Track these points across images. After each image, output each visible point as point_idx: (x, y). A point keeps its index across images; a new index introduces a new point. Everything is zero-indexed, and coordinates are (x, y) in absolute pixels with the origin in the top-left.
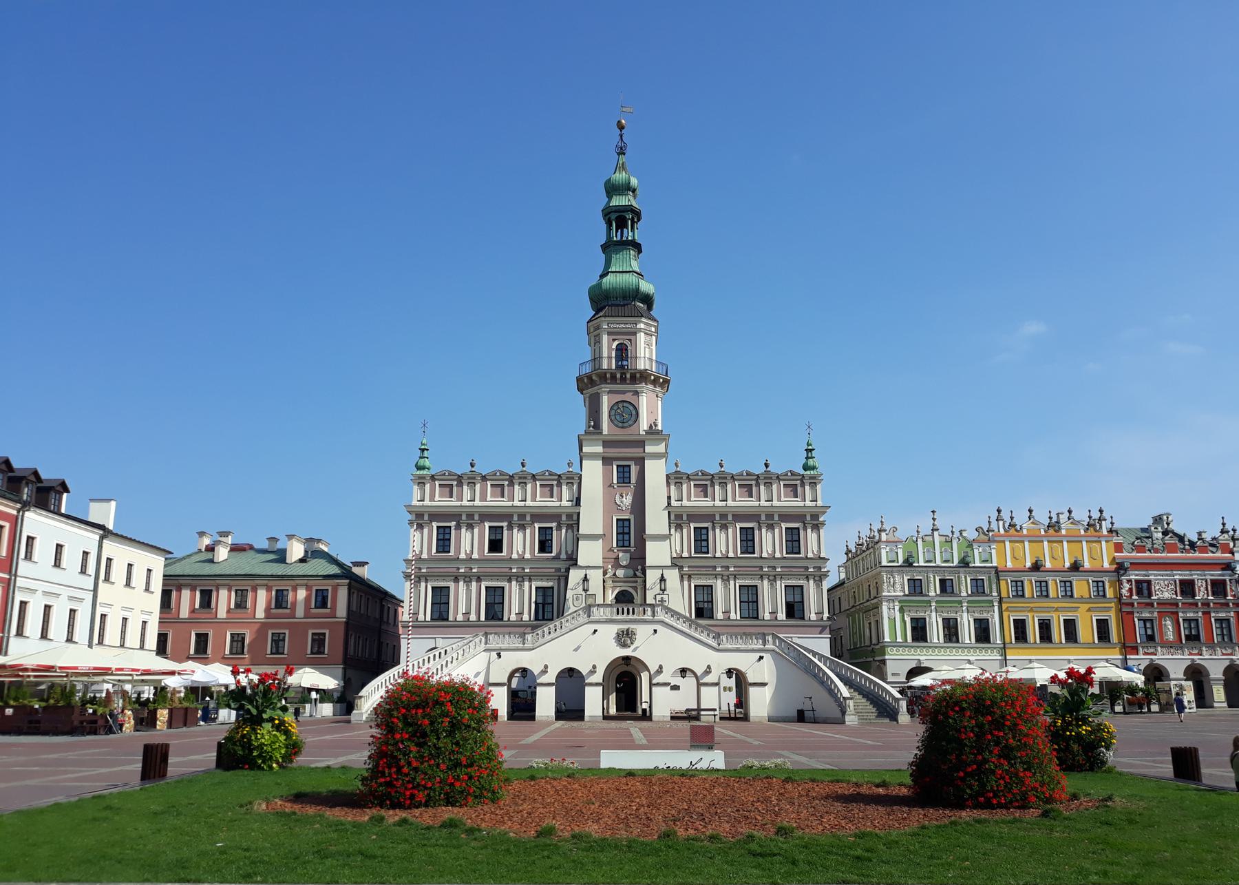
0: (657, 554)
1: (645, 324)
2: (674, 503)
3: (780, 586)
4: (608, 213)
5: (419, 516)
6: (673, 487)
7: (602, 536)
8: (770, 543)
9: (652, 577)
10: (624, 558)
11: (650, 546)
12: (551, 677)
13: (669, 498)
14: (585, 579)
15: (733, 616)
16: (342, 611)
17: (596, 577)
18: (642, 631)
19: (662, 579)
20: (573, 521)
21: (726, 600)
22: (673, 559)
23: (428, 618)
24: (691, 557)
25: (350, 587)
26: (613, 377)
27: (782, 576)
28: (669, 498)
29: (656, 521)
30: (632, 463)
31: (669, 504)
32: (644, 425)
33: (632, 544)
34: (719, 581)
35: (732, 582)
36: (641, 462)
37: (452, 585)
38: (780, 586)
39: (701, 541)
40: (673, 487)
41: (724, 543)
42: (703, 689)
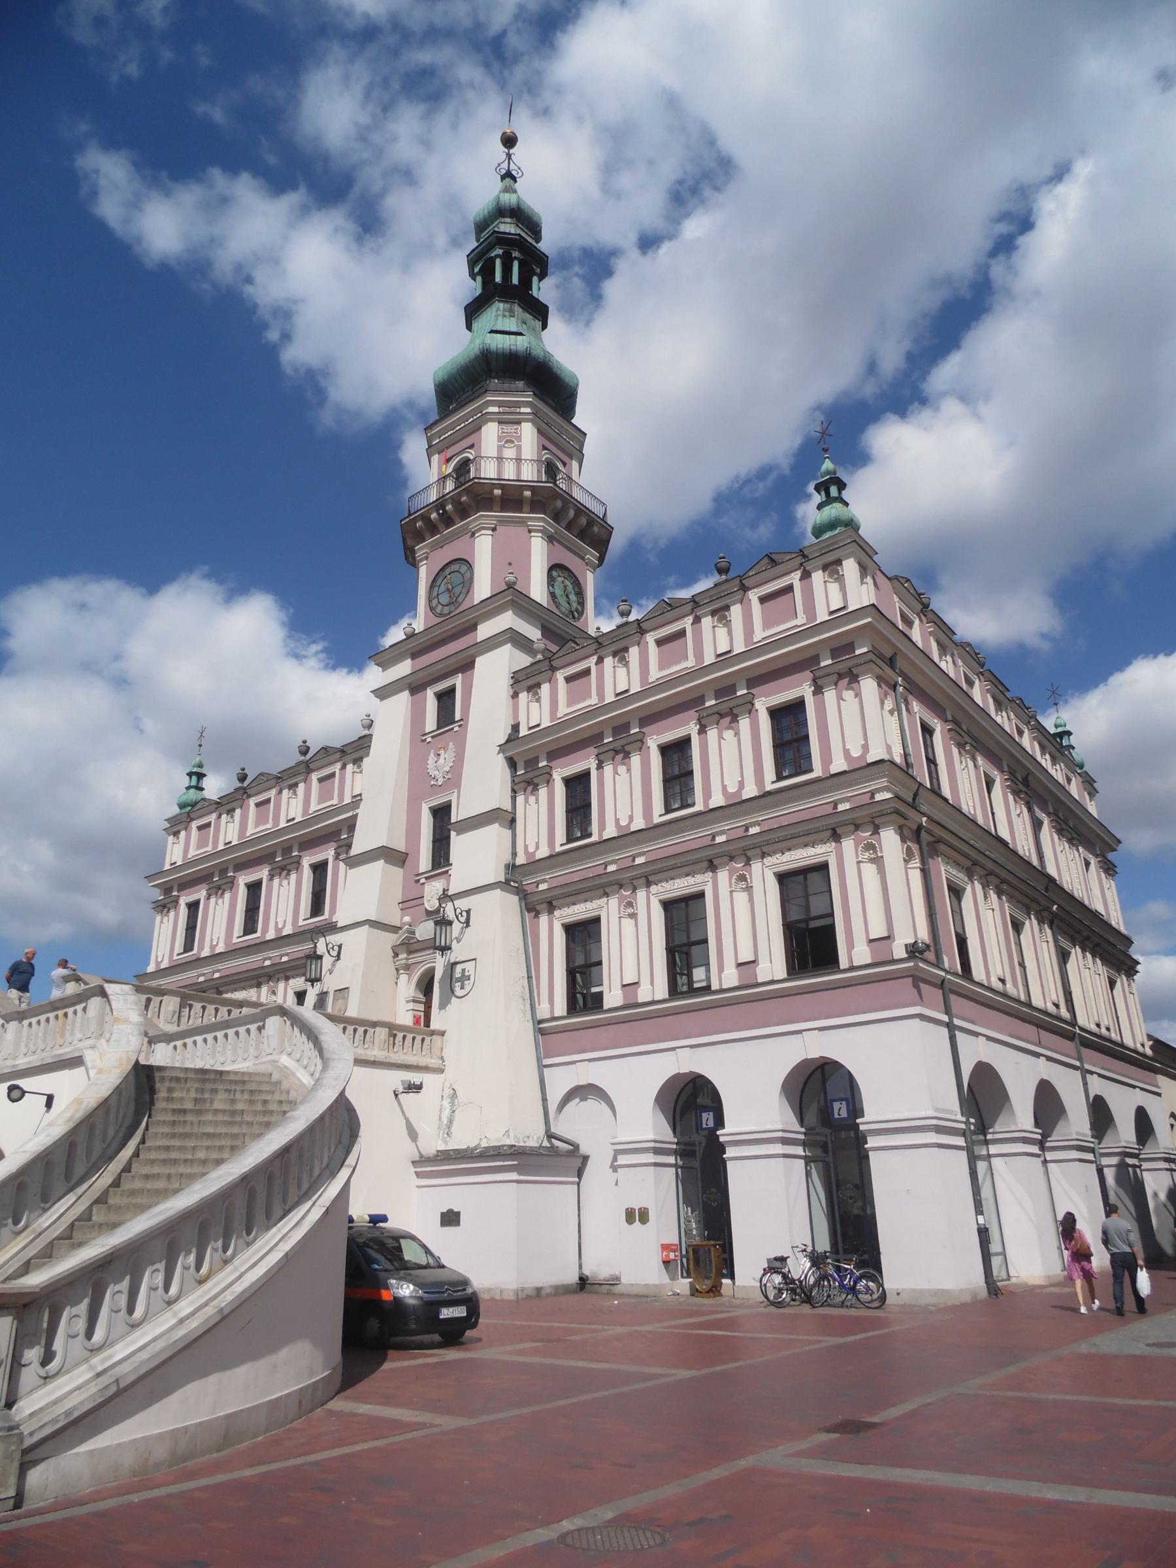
1: (500, 404)
3: (764, 875)
6: (523, 696)
7: (395, 857)
8: (734, 760)
13: (516, 728)
21: (633, 951)
22: (511, 868)
26: (425, 518)
28: (516, 728)
30: (458, 680)
32: (482, 589)
36: (467, 666)
38: (764, 875)
41: (627, 795)
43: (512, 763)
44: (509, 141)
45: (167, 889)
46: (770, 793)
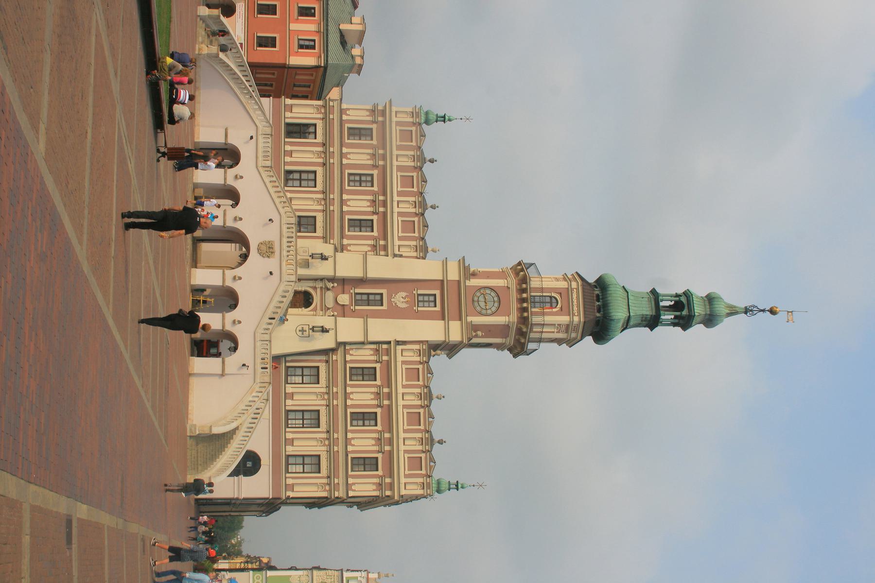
0: (349, 329)
2: (399, 348)
4: (687, 294)
5: (383, 113)
8: (363, 442)
9: (326, 321)
10: (344, 299)
11: (358, 322)
12: (231, 182)
13: (404, 343)
14: (324, 258)
15: (289, 402)
16: (296, 60)
17: (323, 269)
18: (272, 263)
19: (324, 330)
20: (381, 248)
21: (305, 396)
22: (345, 344)
23: (288, 121)
24: (346, 362)
25: (317, 67)
26: (524, 291)
27: (329, 451)
29: (382, 329)
30: (438, 308)
31: (398, 343)
33: (357, 308)
34: (324, 390)
35: (324, 402)
37: (320, 139)
39: (366, 374)
40: (417, 347)
41: (362, 396)
42: (220, 272)
43: (389, 343)
44: (772, 312)
45: (383, 113)
46: (347, 455)
